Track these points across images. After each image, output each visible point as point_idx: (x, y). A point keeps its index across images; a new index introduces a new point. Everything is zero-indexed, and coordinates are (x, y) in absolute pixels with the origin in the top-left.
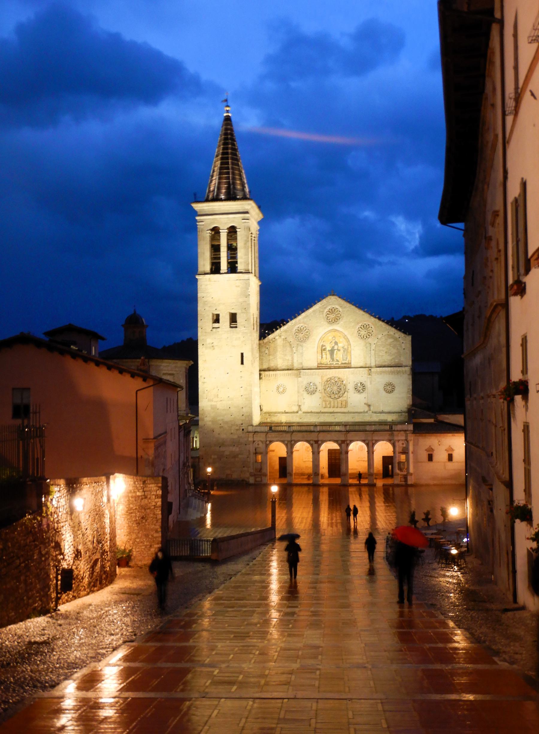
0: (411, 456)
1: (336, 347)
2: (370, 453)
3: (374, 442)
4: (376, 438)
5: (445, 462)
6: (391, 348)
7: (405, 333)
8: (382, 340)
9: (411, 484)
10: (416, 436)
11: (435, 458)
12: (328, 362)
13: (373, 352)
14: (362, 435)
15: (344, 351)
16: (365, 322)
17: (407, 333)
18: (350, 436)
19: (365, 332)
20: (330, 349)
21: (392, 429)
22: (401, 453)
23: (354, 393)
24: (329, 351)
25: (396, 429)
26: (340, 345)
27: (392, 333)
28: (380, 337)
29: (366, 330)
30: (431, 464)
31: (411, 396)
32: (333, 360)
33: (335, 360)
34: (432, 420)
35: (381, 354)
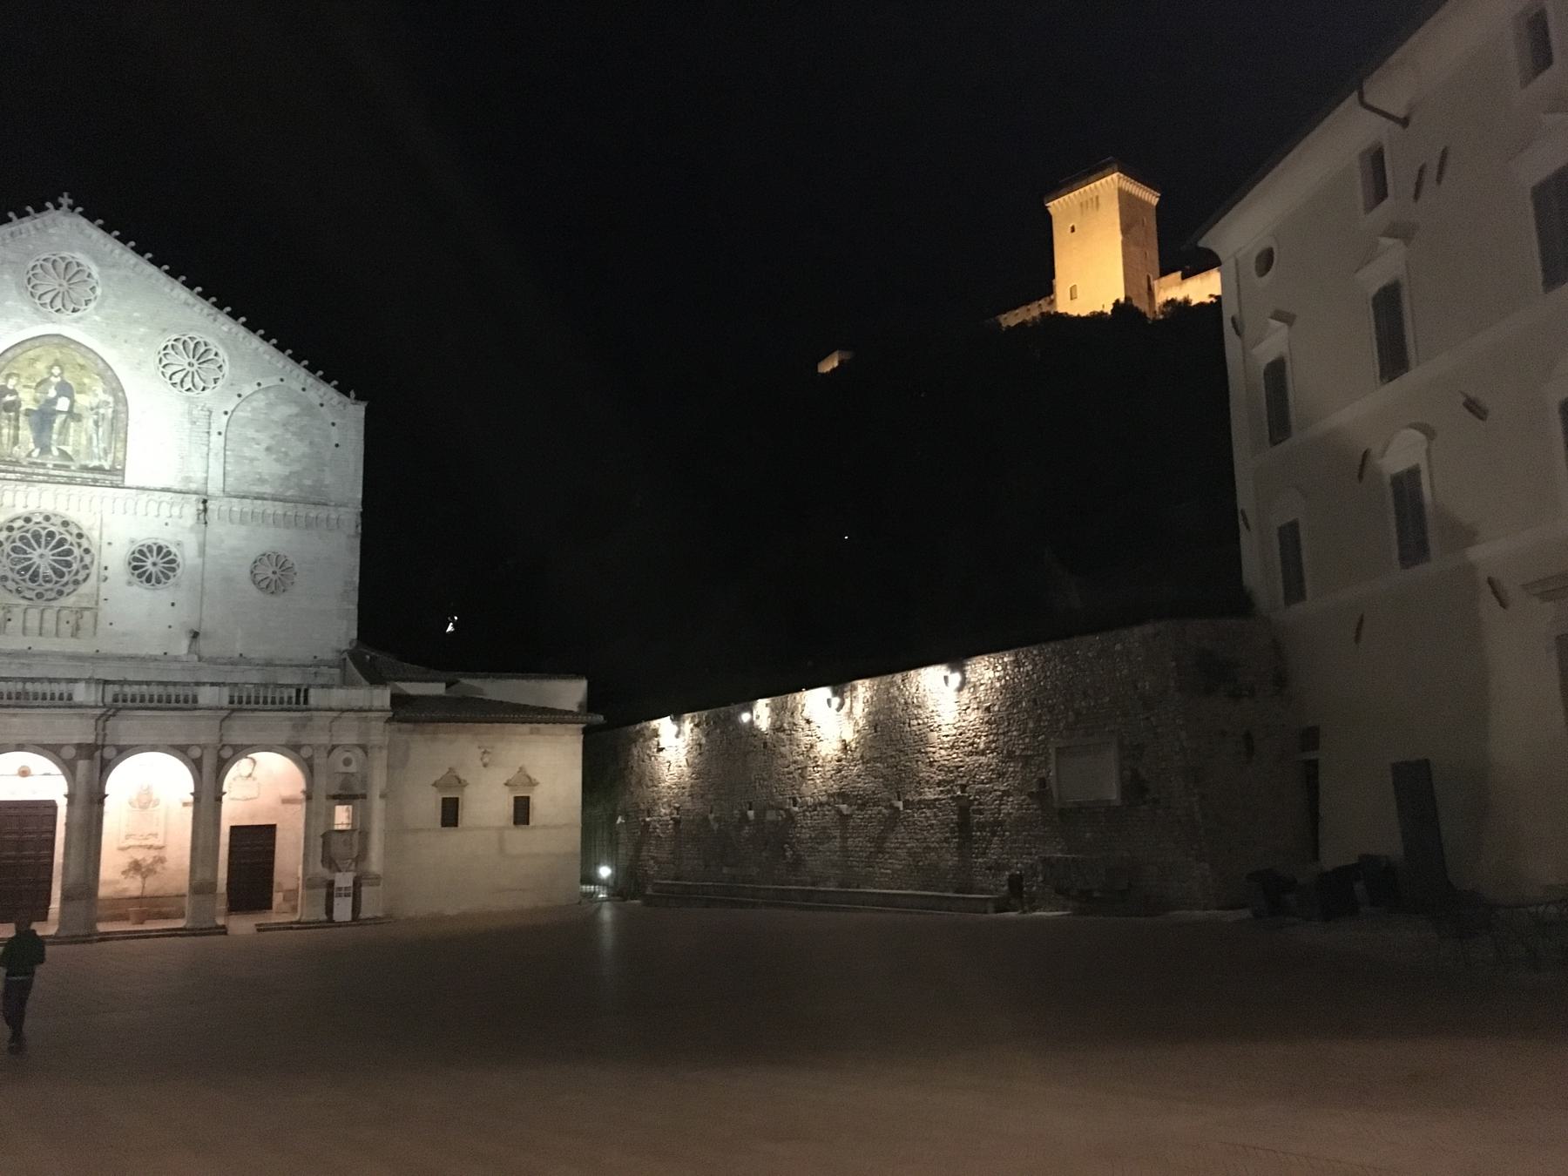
0: (377, 805)
1: (63, 404)
2: (207, 799)
3: (226, 753)
4: (236, 737)
5: (501, 829)
6: (289, 436)
7: (343, 389)
8: (254, 404)
9: (376, 918)
10: (400, 730)
11: (466, 815)
12: (24, 454)
13: (217, 442)
14: (175, 724)
15: (96, 423)
16: (191, 330)
17: (352, 394)
18: (124, 728)
19: (190, 364)
20: (35, 408)
21: (306, 701)
22: (334, 797)
23: (130, 583)
24: (28, 413)
25: (324, 704)
26: (82, 400)
27: (297, 387)
28: (247, 390)
29: (194, 361)
30: (452, 835)
31: (354, 608)
32: (45, 449)
33: (55, 452)
34: (438, 689)
35: (248, 452)
